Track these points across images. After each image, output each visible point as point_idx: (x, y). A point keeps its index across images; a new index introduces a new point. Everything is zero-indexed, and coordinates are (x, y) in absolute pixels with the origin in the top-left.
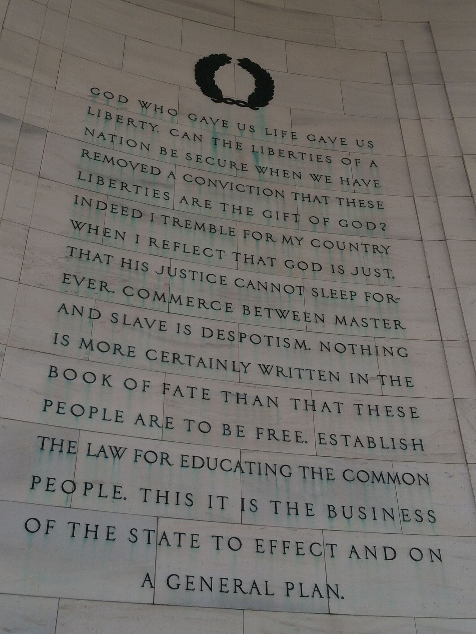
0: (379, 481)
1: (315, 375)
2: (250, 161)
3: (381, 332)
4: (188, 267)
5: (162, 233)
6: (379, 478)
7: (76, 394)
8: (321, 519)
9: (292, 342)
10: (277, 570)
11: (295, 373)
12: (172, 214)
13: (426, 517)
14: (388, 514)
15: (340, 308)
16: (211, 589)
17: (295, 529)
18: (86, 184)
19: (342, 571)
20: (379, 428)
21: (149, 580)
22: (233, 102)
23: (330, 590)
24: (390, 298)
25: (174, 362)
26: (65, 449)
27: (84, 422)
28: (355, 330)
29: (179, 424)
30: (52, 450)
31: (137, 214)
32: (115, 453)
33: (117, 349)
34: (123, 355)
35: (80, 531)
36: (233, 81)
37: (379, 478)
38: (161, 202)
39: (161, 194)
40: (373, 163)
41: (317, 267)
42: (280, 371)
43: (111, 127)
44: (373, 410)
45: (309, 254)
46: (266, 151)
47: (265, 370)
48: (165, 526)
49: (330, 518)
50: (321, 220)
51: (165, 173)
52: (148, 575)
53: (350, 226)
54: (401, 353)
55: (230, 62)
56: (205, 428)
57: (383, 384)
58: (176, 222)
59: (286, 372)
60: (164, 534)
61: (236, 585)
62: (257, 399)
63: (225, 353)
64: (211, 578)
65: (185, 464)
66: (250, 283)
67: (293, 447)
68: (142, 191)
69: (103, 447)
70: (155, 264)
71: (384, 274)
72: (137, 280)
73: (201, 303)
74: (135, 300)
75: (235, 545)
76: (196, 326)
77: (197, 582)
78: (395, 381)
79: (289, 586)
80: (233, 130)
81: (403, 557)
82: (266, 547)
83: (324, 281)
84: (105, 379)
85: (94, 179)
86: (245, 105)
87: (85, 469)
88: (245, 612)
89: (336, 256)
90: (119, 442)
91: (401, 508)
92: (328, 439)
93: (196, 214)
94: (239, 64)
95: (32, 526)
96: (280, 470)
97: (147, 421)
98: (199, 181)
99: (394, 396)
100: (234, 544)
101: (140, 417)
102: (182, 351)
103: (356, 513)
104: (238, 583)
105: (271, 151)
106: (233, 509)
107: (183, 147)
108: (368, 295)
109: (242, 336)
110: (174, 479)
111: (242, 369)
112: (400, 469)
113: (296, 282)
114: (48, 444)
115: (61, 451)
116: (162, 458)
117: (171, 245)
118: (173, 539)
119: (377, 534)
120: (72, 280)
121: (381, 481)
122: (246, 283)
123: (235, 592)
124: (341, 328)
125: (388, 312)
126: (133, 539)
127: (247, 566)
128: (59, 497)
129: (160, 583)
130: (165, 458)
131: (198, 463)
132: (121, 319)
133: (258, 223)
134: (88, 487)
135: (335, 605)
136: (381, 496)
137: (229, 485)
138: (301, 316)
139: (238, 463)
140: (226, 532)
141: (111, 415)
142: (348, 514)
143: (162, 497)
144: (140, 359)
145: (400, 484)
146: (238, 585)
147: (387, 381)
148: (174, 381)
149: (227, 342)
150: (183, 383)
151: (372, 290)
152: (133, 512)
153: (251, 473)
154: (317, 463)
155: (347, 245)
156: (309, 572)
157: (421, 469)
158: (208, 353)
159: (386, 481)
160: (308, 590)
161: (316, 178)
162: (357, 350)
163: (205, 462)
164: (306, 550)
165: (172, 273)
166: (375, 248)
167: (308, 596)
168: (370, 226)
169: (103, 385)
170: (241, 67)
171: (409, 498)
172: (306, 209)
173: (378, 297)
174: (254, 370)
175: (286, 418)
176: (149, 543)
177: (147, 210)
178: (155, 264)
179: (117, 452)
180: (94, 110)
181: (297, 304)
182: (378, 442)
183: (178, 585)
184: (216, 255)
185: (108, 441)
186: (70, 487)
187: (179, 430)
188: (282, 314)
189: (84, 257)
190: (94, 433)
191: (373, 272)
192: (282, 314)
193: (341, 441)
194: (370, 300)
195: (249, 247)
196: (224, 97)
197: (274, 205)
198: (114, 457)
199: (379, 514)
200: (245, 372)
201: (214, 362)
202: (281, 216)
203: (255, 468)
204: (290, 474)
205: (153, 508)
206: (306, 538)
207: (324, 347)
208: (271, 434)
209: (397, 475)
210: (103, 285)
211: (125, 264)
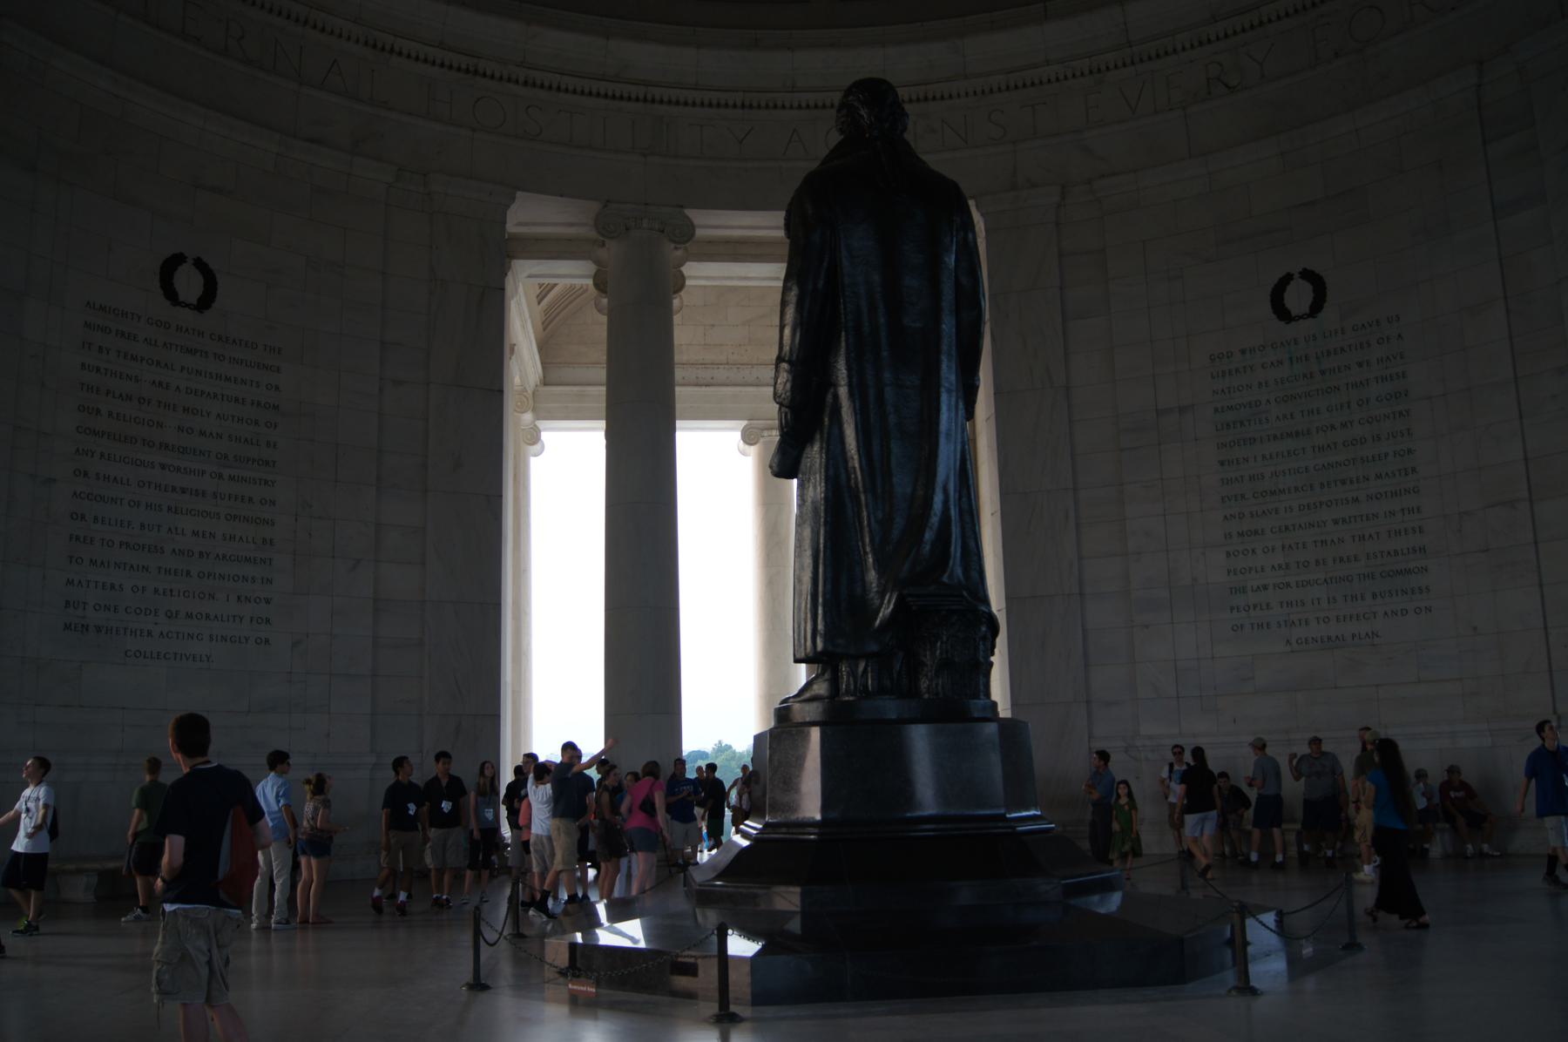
14: (1404, 592)
24: (1410, 451)
31: (1253, 441)
33: (1256, 532)
36: (1298, 297)
37: (1399, 573)
42: (1344, 521)
47: (1336, 522)
58: (1275, 437)
73: (1296, 489)
75: (1327, 620)
78: (1411, 511)
79: (1354, 636)
143: (1289, 604)
161: (1360, 365)
163: (1308, 582)
166: (1401, 413)
207: (1369, 497)
208: (1341, 560)
210: (1243, 496)
211: (1252, 478)
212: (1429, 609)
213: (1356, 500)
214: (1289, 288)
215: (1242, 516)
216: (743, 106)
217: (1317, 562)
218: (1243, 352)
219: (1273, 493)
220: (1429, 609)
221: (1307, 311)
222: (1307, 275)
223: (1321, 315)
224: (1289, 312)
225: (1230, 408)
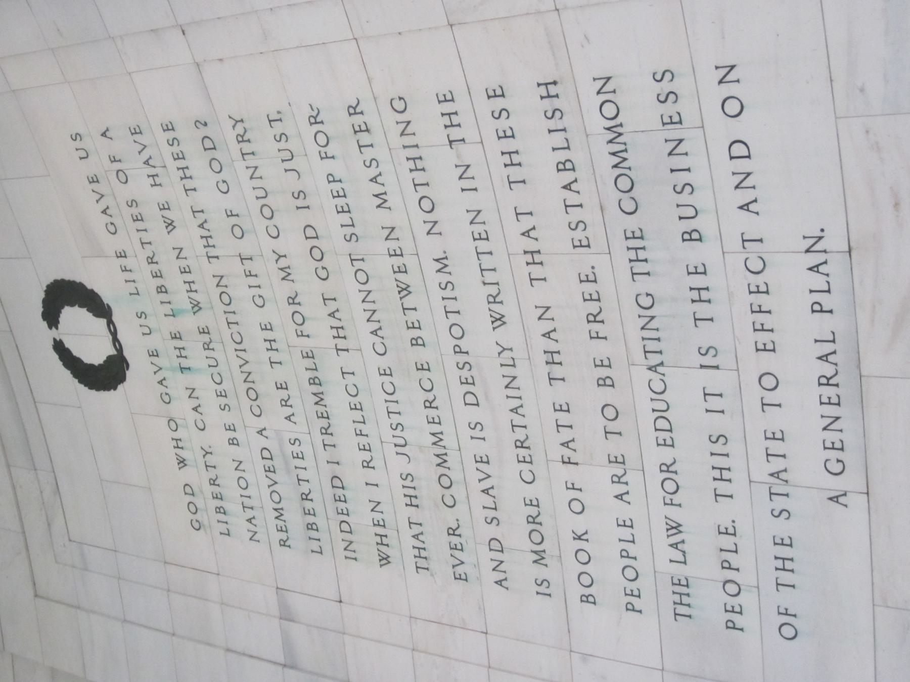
0: (625, 159)
1: (483, 246)
3: (376, 137)
4: (385, 422)
6: (620, 159)
7: (608, 571)
9: (444, 278)
10: (797, 329)
11: (490, 277)
12: (318, 438)
13: (666, 87)
14: (675, 147)
15: (362, 198)
16: (837, 418)
17: (730, 295)
18: (327, 548)
19: (782, 228)
20: (539, 153)
21: (837, 497)
22: (114, 334)
23: (813, 249)
24: (314, 120)
25: (528, 448)
26: (684, 590)
28: (388, 179)
30: (689, 605)
32: (674, 531)
33: (533, 520)
34: (539, 514)
35: (785, 577)
37: (620, 159)
38: (307, 449)
39: (296, 449)
40: (104, 134)
41: (310, 233)
42: (493, 299)
43: (233, 506)
44: (511, 159)
45: (294, 245)
46: (163, 297)
47: (499, 321)
48: (761, 470)
49: (703, 239)
50: (233, 220)
51: (264, 443)
52: (831, 499)
53: (223, 176)
54: (400, 105)
55: (61, 340)
56: (611, 413)
57: (463, 140)
58: (325, 431)
59: (493, 290)
60: (772, 475)
61: (828, 384)
62: (547, 335)
63: (491, 377)
64: (822, 416)
65: (669, 442)
66: (374, 333)
67: (605, 286)
68: (303, 475)
69: (671, 545)
71: (278, 128)
72: (428, 489)
74: (458, 491)
75: (769, 382)
77: (831, 436)
78: (451, 120)
80: (154, 342)
81: (738, 128)
82: (763, 337)
83: (331, 226)
84: (579, 538)
85: (313, 534)
86: (110, 322)
87: (703, 568)
88: (863, 373)
89: (280, 201)
90: (660, 528)
91: (661, 127)
92: (579, 234)
93: (303, 403)
94: (57, 328)
95: (788, 631)
96: (647, 305)
97: (621, 489)
99: (476, 117)
100: (769, 382)
101: (619, 497)
102: (510, 438)
103: (685, 198)
104: (824, 381)
105: (161, 290)
108: (323, 155)
109: (458, 350)
111: (506, 354)
112: (597, 124)
114: (681, 610)
115: (688, 595)
116: (668, 471)
117: (363, 441)
118: (777, 464)
119: (711, 171)
120: (460, 570)
121: (623, 155)
122: (377, 340)
123: (837, 385)
124: (393, 200)
125: (338, 123)
126: (785, 514)
127: (799, 366)
128: (747, 600)
129: (837, 484)
130: (667, 468)
131: (662, 424)
132: (491, 514)
133: (277, 313)
134: (727, 566)
135: (835, 242)
136: (647, 155)
137: (685, 387)
138: (397, 261)
139: (650, 369)
140: (753, 394)
141: (626, 533)
142: (690, 212)
143: (721, 474)
145: (621, 125)
146: (826, 381)
147: (455, 133)
148: (558, 452)
149: (474, 372)
151: (313, 150)
152: (748, 510)
153: (661, 352)
154: (622, 256)
155: (257, 183)
156: (791, 280)
157: (588, 90)
158: (498, 392)
159: (622, 147)
160: (819, 282)
162: (420, 177)
163: (661, 414)
164: (759, 280)
165: (402, 442)
167: (828, 283)
168: (209, 145)
169: (587, 540)
170: (59, 326)
171: (641, 112)
172: (225, 244)
173: (322, 139)
174: (505, 335)
175: (562, 291)
176: (787, 495)
177: (327, 471)
178: (398, 465)
179: (673, 528)
180: (223, 528)
181: (381, 266)
182: (562, 156)
183: (838, 461)
184: (350, 379)
185: (662, 541)
186: (732, 586)
189: (423, 553)
191: (282, 145)
192: (404, 290)
193: (575, 215)
194: (330, 150)
196: (115, 353)
197: (240, 290)
198: (680, 532)
199: (678, 162)
200: (511, 349)
201: (510, 392)
202: (252, 281)
203: (651, 346)
204: (648, 295)
205: (738, 487)
206: (741, 280)
208: (594, 318)
209: (608, 129)
210: (452, 532)
211: (412, 502)
212: (727, 73)
213: (442, 263)
214: (75, 353)
215: (496, 545)
217: (603, 382)
220: (727, 73)
221: (103, 322)
223: (107, 297)
224: (110, 358)
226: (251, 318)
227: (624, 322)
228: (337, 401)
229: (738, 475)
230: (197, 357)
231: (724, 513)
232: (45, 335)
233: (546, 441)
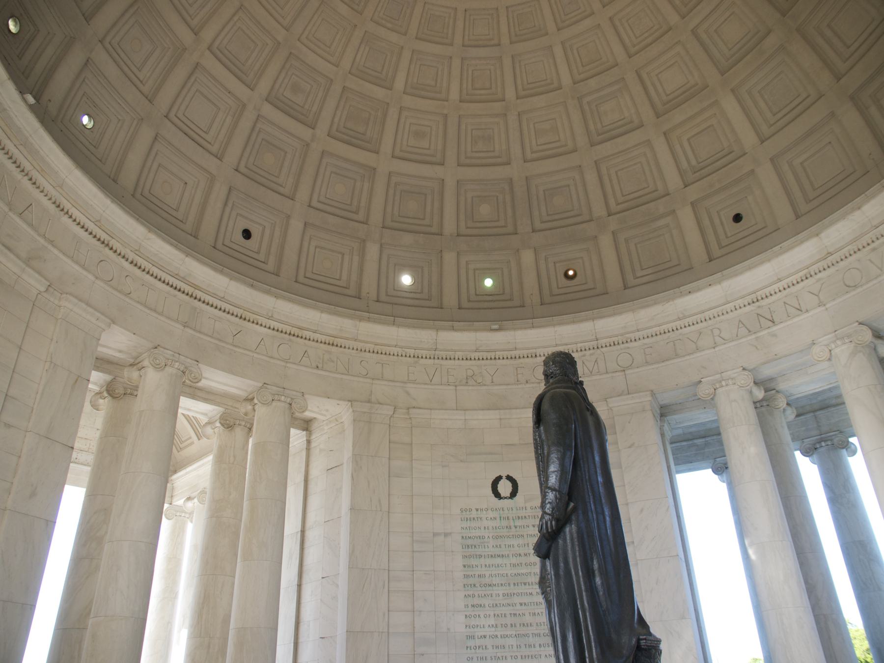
2: (512, 524)
5: (489, 561)
7: (473, 622)
8: (538, 648)
27: (476, 629)
29: (499, 626)
31: (480, 556)
36: (505, 488)
38: (487, 550)
43: (469, 524)
47: (521, 604)
48: (498, 655)
56: (506, 626)
70: (487, 574)
74: (484, 588)
76: (501, 593)
80: (506, 511)
87: (478, 642)
93: (497, 551)
98: (497, 537)
102: (498, 602)
106: (515, 648)
107: (491, 524)
110: (500, 642)
113: (529, 571)
130: (497, 636)
140: (514, 654)
143: (497, 647)
144: (487, 608)
148: (496, 613)
150: (499, 613)
174: (518, 605)
178: (487, 574)
187: (499, 628)
188: (525, 584)
190: (479, 632)
192: (525, 584)
195: (514, 560)
205: (495, 650)
211: (479, 576)
213: (531, 594)
216: (241, 317)
218: (477, 510)
219: (490, 585)
222: (509, 478)
225: (470, 538)
226: (515, 542)
227: (524, 630)
228: (499, 561)
229: (497, 650)
230: (505, 523)
231: (489, 647)
232: (504, 475)
233: (498, 611)
